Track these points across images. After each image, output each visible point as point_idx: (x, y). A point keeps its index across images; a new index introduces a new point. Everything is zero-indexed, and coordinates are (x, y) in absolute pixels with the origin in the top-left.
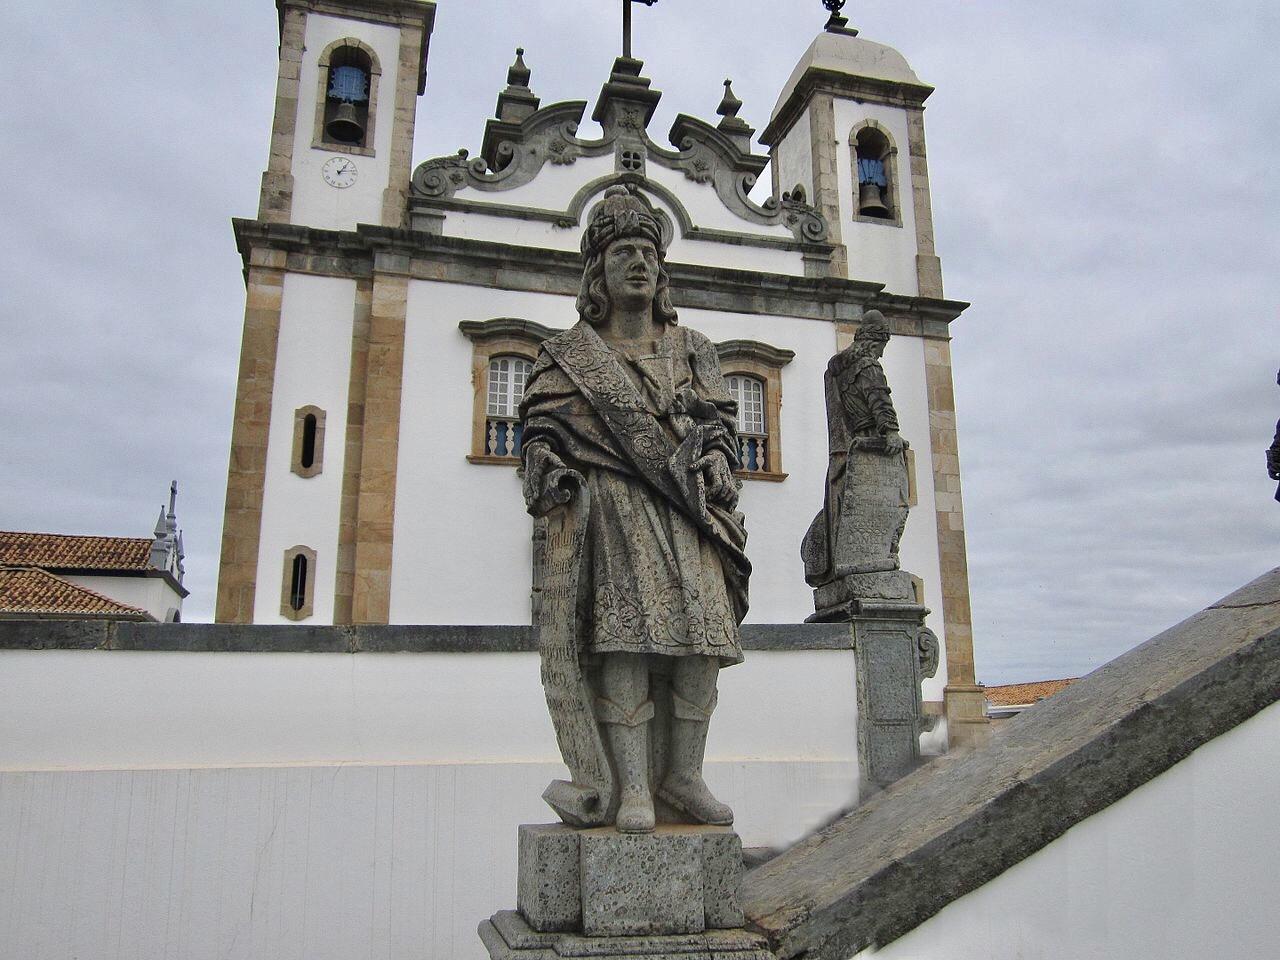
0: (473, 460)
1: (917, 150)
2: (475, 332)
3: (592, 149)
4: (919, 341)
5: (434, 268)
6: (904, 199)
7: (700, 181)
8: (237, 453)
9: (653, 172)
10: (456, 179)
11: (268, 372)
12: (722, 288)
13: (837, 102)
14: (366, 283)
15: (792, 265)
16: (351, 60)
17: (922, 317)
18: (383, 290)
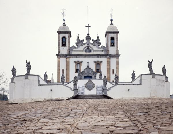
0: (75, 73)
1: (117, 39)
2: (75, 62)
3: (85, 44)
4: (115, 59)
5: (72, 57)
6: (115, 44)
7: (95, 45)
8: (58, 73)
9: (90, 45)
10: (73, 48)
11: (60, 66)
12: (96, 56)
13: (109, 35)
14: (66, 58)
15: (103, 53)
16: (64, 38)
17: (116, 56)
18: (68, 59)
